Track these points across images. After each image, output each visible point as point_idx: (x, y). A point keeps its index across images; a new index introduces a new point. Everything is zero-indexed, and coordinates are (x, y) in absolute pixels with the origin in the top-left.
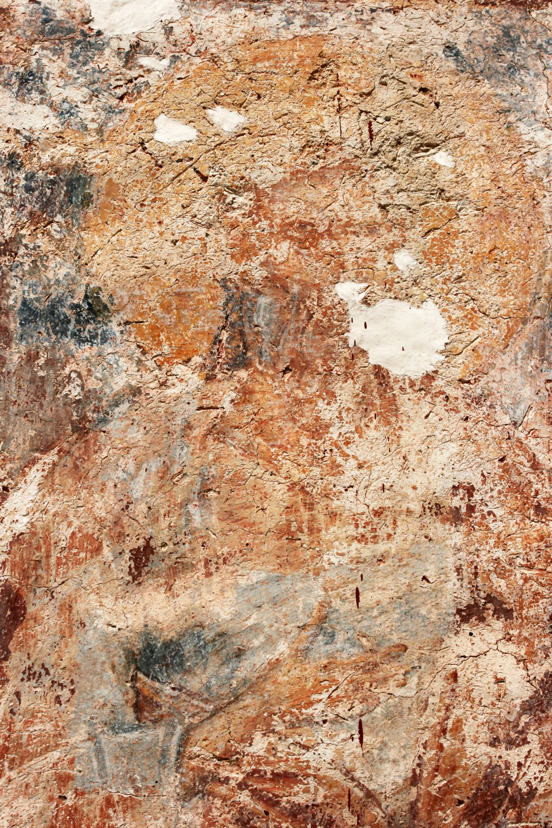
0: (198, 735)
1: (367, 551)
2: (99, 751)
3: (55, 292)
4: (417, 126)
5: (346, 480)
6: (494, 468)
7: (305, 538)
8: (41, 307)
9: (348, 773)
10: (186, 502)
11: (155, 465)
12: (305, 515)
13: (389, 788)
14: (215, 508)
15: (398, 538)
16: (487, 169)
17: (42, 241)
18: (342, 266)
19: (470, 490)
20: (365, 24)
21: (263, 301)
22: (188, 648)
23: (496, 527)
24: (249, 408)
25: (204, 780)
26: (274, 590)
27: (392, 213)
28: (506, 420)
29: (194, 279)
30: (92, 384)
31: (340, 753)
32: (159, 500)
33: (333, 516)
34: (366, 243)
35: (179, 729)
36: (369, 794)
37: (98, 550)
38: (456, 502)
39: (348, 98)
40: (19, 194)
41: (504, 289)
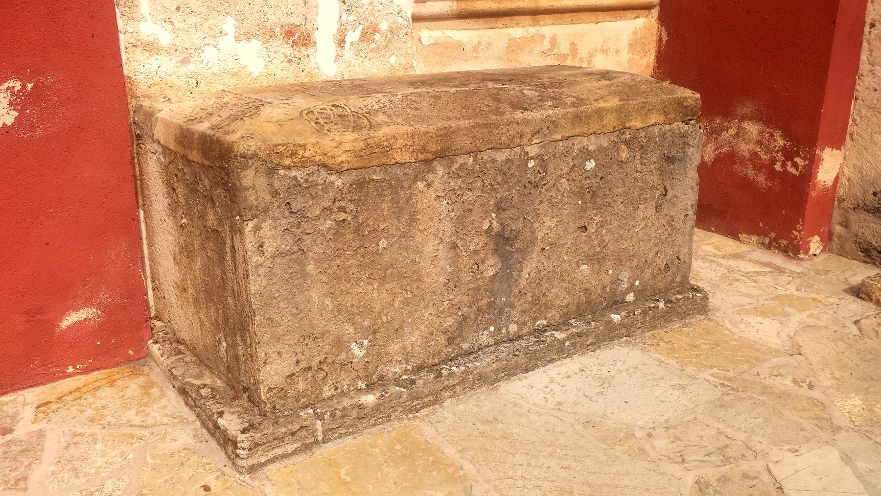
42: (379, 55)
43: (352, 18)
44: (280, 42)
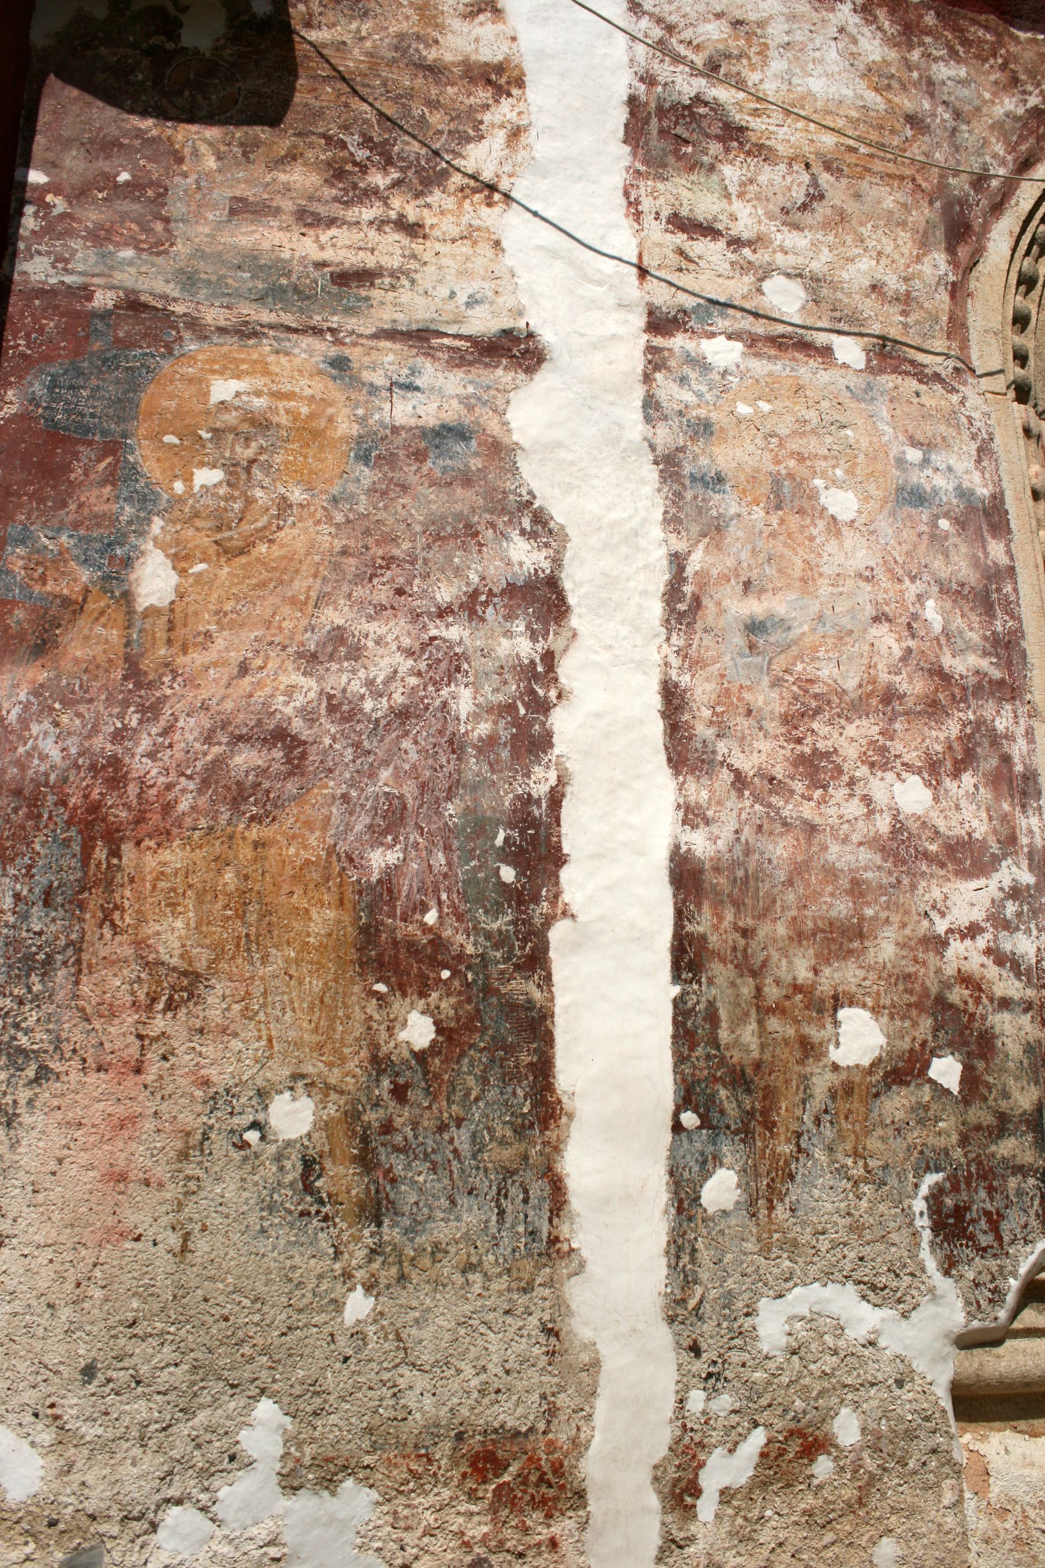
0: (774, 661)
1: (835, 590)
3: (704, 470)
8: (698, 476)
11: (749, 547)
17: (696, 448)
19: (872, 569)
20: (815, 374)
21: (786, 483)
22: (769, 624)
23: (883, 585)
26: (800, 603)
30: (721, 511)
32: (751, 562)
33: (821, 575)
34: (824, 464)
37: (729, 580)
38: (867, 573)
39: (810, 404)
40: (685, 428)
41: (878, 488)
42: (829, 1537)
43: (725, 1402)
44: (446, 1493)
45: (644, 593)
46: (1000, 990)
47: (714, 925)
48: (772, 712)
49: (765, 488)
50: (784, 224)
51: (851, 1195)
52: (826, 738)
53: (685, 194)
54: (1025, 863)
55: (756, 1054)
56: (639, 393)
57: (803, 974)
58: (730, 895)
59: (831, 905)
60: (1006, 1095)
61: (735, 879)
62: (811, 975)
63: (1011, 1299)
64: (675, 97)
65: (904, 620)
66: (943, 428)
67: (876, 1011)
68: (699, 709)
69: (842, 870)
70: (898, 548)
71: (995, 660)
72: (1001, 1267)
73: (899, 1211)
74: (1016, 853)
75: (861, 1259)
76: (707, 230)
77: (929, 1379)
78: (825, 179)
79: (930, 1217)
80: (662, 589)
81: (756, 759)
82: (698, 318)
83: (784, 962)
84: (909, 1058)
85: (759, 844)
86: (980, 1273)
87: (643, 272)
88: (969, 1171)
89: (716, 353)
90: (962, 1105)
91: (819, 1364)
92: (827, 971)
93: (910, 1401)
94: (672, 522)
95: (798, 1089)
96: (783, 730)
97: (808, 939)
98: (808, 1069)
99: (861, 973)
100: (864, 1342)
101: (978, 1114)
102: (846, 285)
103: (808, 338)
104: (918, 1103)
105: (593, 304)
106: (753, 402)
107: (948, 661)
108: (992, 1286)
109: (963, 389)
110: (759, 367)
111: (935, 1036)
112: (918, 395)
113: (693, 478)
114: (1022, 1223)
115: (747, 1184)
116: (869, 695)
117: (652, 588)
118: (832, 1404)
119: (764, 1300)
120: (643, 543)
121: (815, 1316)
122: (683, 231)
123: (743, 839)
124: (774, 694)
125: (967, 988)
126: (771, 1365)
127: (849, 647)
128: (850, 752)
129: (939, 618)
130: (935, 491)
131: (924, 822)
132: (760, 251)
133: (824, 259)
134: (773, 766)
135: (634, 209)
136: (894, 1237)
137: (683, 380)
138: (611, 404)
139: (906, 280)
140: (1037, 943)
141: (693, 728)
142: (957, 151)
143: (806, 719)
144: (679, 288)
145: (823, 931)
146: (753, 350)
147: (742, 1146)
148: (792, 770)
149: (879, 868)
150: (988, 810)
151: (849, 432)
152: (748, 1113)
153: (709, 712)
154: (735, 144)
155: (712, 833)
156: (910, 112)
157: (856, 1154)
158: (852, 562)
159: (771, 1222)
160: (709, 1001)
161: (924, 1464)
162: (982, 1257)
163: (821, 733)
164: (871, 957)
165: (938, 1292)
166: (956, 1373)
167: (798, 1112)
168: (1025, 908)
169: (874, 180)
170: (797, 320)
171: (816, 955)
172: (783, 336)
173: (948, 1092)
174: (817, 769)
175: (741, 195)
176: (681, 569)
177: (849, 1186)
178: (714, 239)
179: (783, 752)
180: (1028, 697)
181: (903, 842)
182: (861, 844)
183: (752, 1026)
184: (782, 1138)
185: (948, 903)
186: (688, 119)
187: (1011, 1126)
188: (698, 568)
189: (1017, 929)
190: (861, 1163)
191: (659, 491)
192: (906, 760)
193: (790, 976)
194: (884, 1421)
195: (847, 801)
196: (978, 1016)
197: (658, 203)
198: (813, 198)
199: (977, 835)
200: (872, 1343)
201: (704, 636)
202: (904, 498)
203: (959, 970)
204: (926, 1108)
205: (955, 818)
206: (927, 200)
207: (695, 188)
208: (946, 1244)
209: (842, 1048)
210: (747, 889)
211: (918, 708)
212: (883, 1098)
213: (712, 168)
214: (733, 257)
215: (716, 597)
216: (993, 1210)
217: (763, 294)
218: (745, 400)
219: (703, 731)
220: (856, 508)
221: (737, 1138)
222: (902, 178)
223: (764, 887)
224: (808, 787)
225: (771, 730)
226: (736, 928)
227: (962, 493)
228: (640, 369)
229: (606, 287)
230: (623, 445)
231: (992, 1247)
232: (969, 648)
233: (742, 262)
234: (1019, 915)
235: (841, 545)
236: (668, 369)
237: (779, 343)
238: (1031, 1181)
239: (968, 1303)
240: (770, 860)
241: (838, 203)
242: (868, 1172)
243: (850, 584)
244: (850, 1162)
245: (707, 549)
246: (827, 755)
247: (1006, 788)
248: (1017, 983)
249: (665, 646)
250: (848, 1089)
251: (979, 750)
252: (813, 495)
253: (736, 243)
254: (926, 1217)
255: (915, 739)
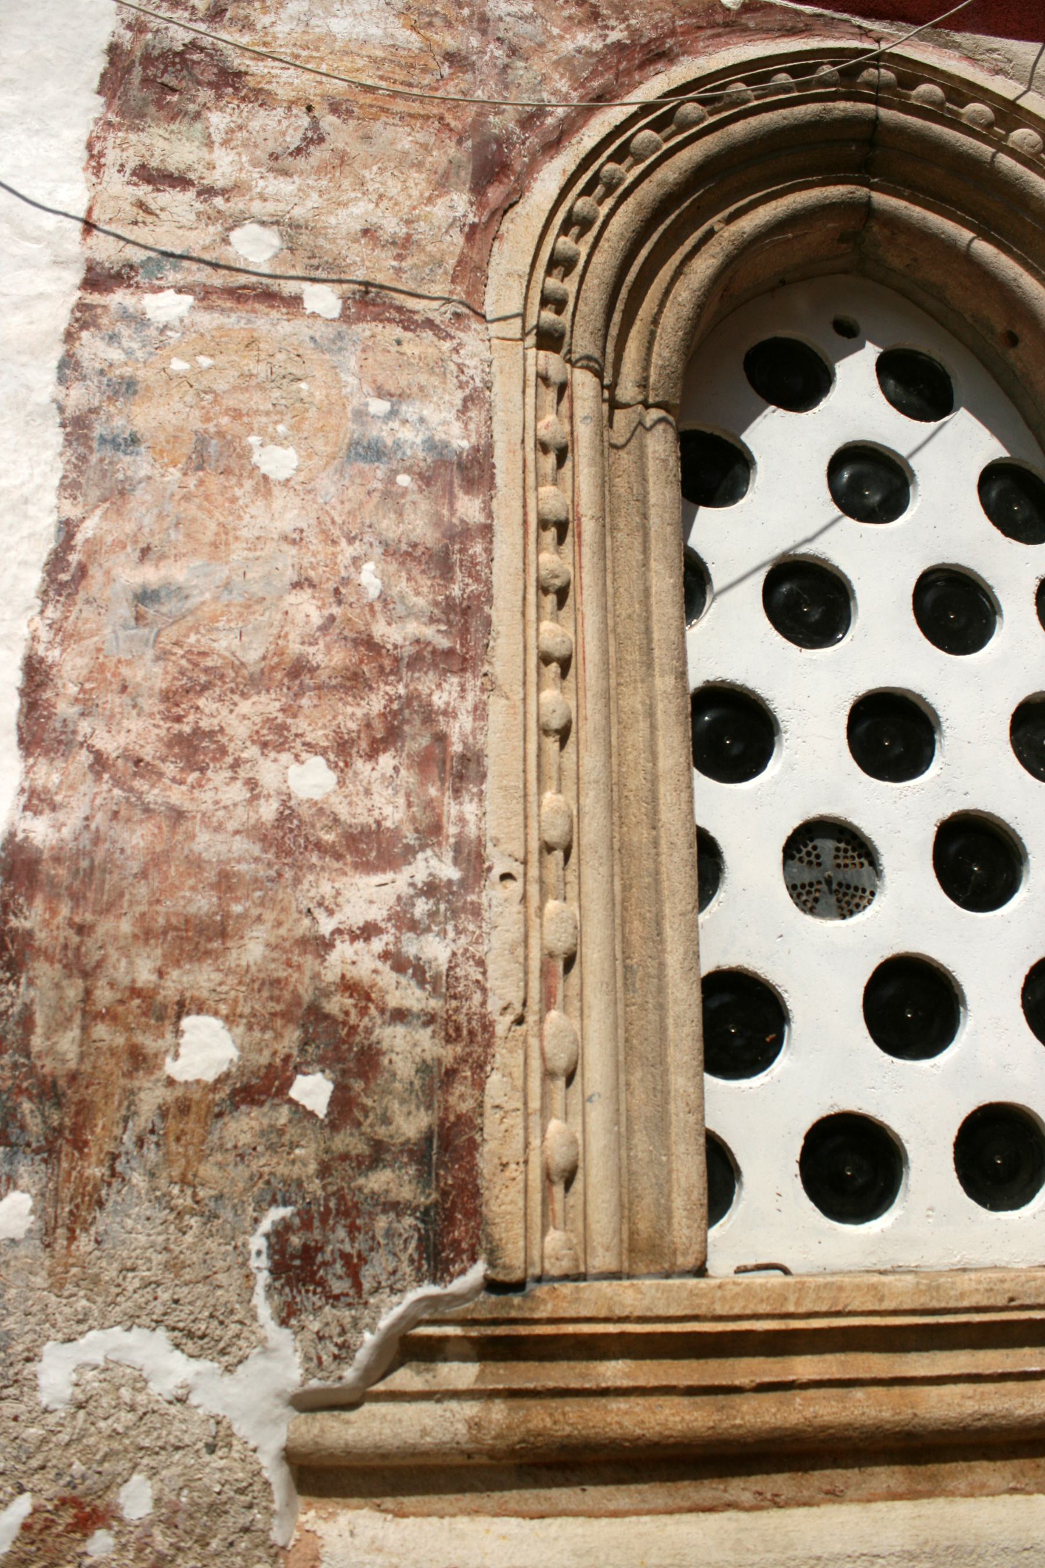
0: (164, 633)
1: (251, 555)
2: (117, 638)
3: (116, 432)
4: (294, 371)
5: (244, 523)
6: (314, 522)
7: (223, 547)
8: (109, 438)
9: (233, 654)
10: (168, 528)
11: (155, 511)
12: (224, 537)
13: (252, 661)
14: (182, 531)
15: (266, 550)
16: (324, 392)
17: (112, 409)
18: (252, 429)
19: (302, 531)
20: (274, 325)
21: (213, 442)
22: (163, 593)
23: (312, 548)
24: (202, 489)
25: (165, 653)
27: (278, 408)
28: (321, 501)
29: (181, 429)
30: (129, 473)
31: (230, 644)
32: (156, 527)
33: (237, 538)
34: (264, 419)
35: (155, 630)
36: (242, 664)
37: (124, 547)
38: (296, 536)
39: (263, 356)
40: (104, 387)
41: (326, 444)
45: (23, 563)
46: (393, 1001)
47: (45, 920)
48: (151, 689)
49: (187, 448)
50: (271, 170)
51: (172, 1227)
52: (212, 715)
53: (160, 144)
54: (449, 855)
55: (72, 1065)
56: (58, 351)
57: (145, 975)
58: (69, 888)
59: (190, 901)
60: (386, 1120)
61: (77, 871)
62: (154, 977)
63: (362, 1356)
64: (166, 44)
65: (331, 585)
66: (423, 378)
67: (230, 1020)
68: (64, 686)
69: (209, 862)
70: (339, 507)
71: (443, 628)
72: (355, 1321)
73: (230, 1248)
74: (439, 844)
75: (176, 1302)
76: (179, 181)
77: (252, 1444)
78: (329, 122)
79: (270, 1257)
80: (44, 558)
81: (122, 740)
82: (146, 272)
83: (124, 962)
84: (266, 1075)
85: (112, 833)
86: (327, 1324)
87: (89, 226)
88: (326, 1207)
89: (158, 308)
90: (327, 1131)
91: (110, 1421)
92: (175, 974)
93: (221, 1470)
94: (69, 487)
95: (120, 1104)
96: (162, 707)
97: (156, 937)
98: (137, 1083)
99: (217, 977)
100: (170, 1398)
101: (347, 1141)
102: (330, 231)
103: (275, 288)
104: (271, 1126)
105: (26, 262)
106: (192, 358)
107: (382, 630)
108: (340, 1340)
109: (461, 335)
110: (207, 320)
111: (302, 1051)
112: (399, 343)
113: (103, 440)
114: (390, 1269)
115: (44, 1209)
116: (273, 669)
117: (33, 558)
118: (119, 1469)
119: (50, 1344)
120: (32, 510)
121: (111, 1366)
122: (149, 182)
123: (93, 826)
124: (158, 669)
125: (351, 996)
126: (51, 1420)
127: (257, 616)
128: (239, 730)
129: (378, 582)
130: (398, 445)
131: (321, 809)
132: (233, 200)
133: (310, 204)
134: (142, 746)
135: (95, 161)
136: (222, 1278)
137: (113, 338)
138: (23, 365)
139: (408, 222)
140: (453, 946)
141: (54, 706)
142: (506, 87)
143: (191, 695)
144: (128, 241)
145: (176, 929)
146: (205, 303)
147: (43, 1167)
148: (164, 751)
149: (257, 860)
150: (408, 795)
151: (303, 385)
152: (54, 1129)
153: (76, 689)
154: (230, 90)
155: (57, 820)
156: (451, 50)
157: (183, 1181)
158: (278, 524)
159: (69, 1254)
160: (25, 1004)
161: (231, 1544)
162: (333, 1306)
163: (207, 711)
164: (232, 959)
165: (271, 1344)
166: (289, 1439)
167: (117, 1131)
168: (442, 907)
169: (391, 121)
170: (265, 269)
171: (164, 956)
172: (245, 287)
173: (312, 1114)
174: (196, 749)
175: (225, 143)
176: (70, 536)
177: (172, 1217)
178: (184, 190)
179: (157, 731)
180: (486, 668)
181: (291, 830)
182: (237, 832)
183: (75, 1033)
184: (94, 1159)
185: (340, 900)
186: (178, 67)
187: (388, 1157)
188: (90, 534)
189: (428, 929)
190: (189, 1192)
191: (61, 454)
192: (308, 739)
193: (128, 979)
194: (185, 1492)
195: (227, 784)
196: (361, 1029)
197: (125, 154)
198: (311, 141)
199: (388, 824)
200: (179, 1400)
201: (85, 607)
202: (357, 454)
203: (343, 976)
204: (281, 1132)
205: (362, 804)
206: (454, 139)
207: (173, 137)
208: (287, 1290)
209: (181, 1061)
210: (91, 881)
211: (334, 682)
212: (226, 1119)
213: (197, 116)
214: (199, 206)
215: (106, 565)
216: (354, 1252)
217: (230, 244)
218: (182, 356)
219: (64, 709)
220: (294, 465)
221: (38, 1157)
222: (427, 118)
223: (111, 880)
224: (182, 770)
225: (147, 708)
226: (71, 924)
227: (431, 445)
228: (63, 327)
229: (44, 244)
230: (30, 408)
231: (347, 1295)
232: (412, 613)
233: (210, 212)
234: (432, 915)
235: (268, 506)
236: (98, 327)
237: (237, 295)
238: (408, 1221)
239: (307, 1358)
240: (122, 850)
241: (340, 145)
242: (197, 1202)
243: (270, 547)
244: (176, 1190)
245: (104, 516)
246: (211, 734)
247: (436, 771)
248: (419, 993)
249: (38, 619)
250: (184, 1107)
251: (406, 728)
252: (246, 454)
253: (207, 192)
254: (264, 1257)
255: (324, 716)
